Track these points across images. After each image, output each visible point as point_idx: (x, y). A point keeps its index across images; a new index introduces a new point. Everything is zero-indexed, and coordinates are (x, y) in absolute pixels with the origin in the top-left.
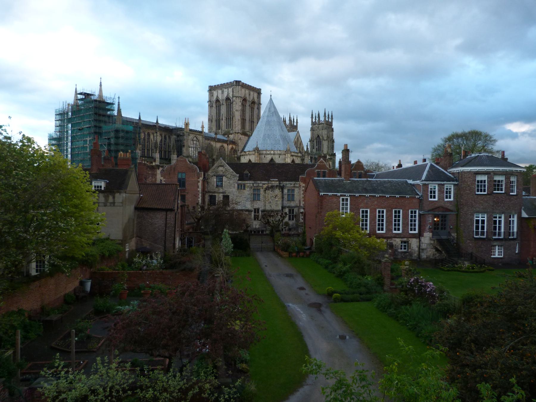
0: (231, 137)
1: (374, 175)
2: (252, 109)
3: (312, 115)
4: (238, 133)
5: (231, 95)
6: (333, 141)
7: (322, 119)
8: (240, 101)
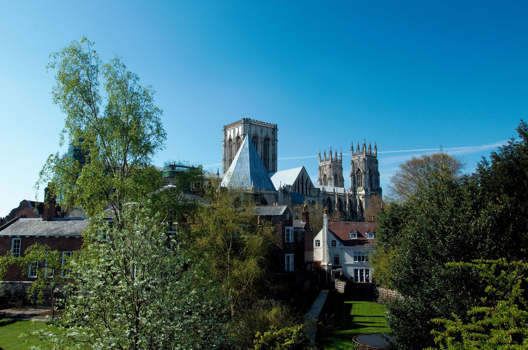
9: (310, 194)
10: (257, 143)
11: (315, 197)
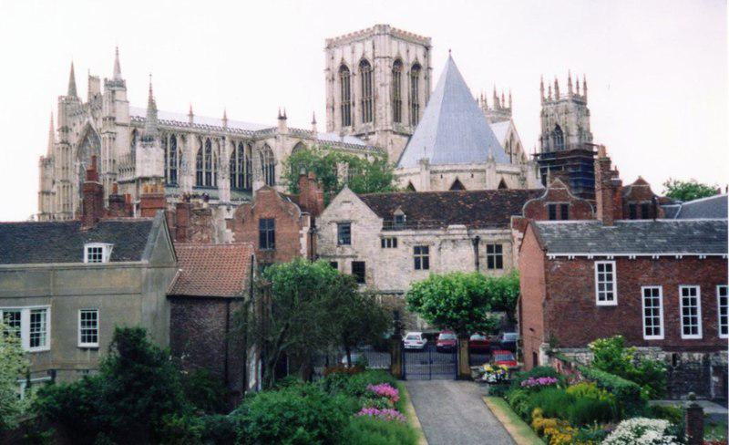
0: (373, 138)
1: (677, 209)
2: (414, 79)
3: (542, 84)
4: (386, 131)
7: (564, 91)
8: (390, 67)
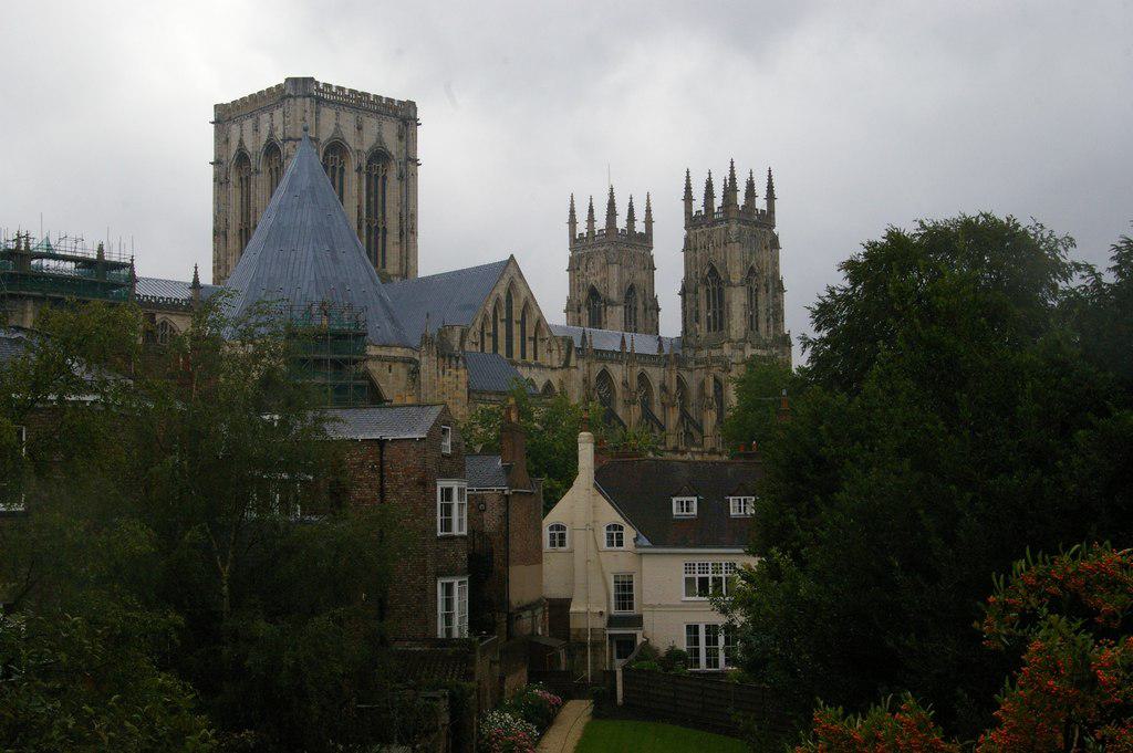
5: (279, 135)
6: (780, 288)
9: (535, 358)
10: (342, 170)
11: (554, 369)
